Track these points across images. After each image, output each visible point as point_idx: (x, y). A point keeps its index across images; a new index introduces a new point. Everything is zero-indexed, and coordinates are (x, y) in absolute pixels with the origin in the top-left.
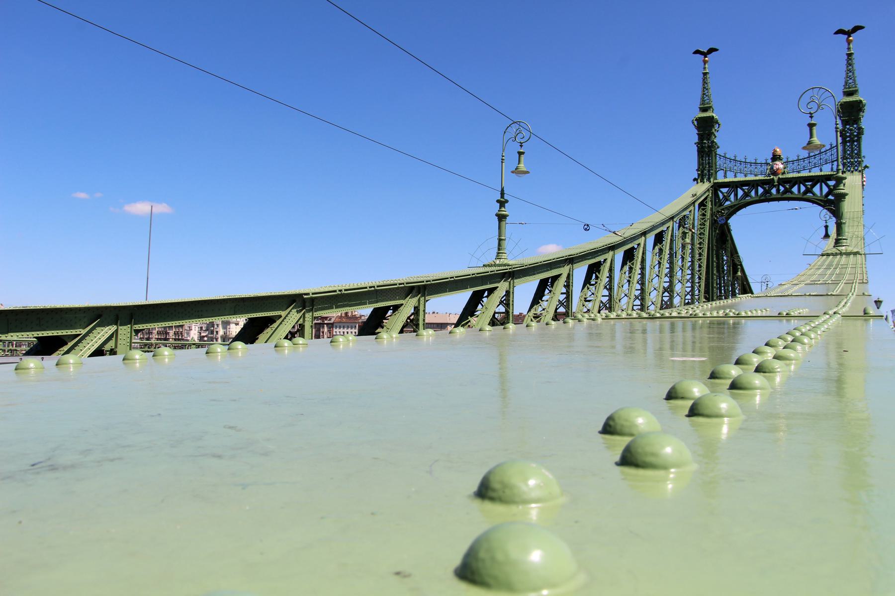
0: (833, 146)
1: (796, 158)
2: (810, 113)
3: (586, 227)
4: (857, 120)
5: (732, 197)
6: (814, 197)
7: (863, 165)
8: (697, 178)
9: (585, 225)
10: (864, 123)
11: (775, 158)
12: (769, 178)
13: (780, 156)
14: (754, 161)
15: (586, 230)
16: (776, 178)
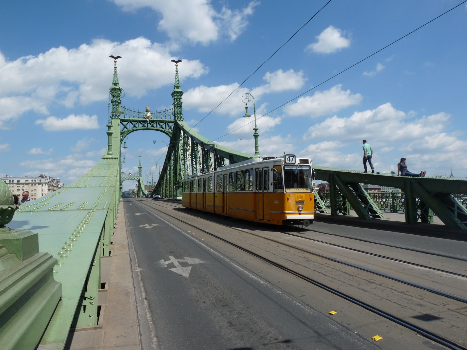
1: (156, 112)
2: (246, 103)
3: (154, 142)
4: (180, 99)
5: (127, 126)
7: (183, 118)
8: (112, 116)
9: (154, 141)
10: (182, 100)
11: (147, 111)
12: (145, 119)
13: (149, 110)
14: (138, 111)
15: (154, 143)
16: (148, 120)
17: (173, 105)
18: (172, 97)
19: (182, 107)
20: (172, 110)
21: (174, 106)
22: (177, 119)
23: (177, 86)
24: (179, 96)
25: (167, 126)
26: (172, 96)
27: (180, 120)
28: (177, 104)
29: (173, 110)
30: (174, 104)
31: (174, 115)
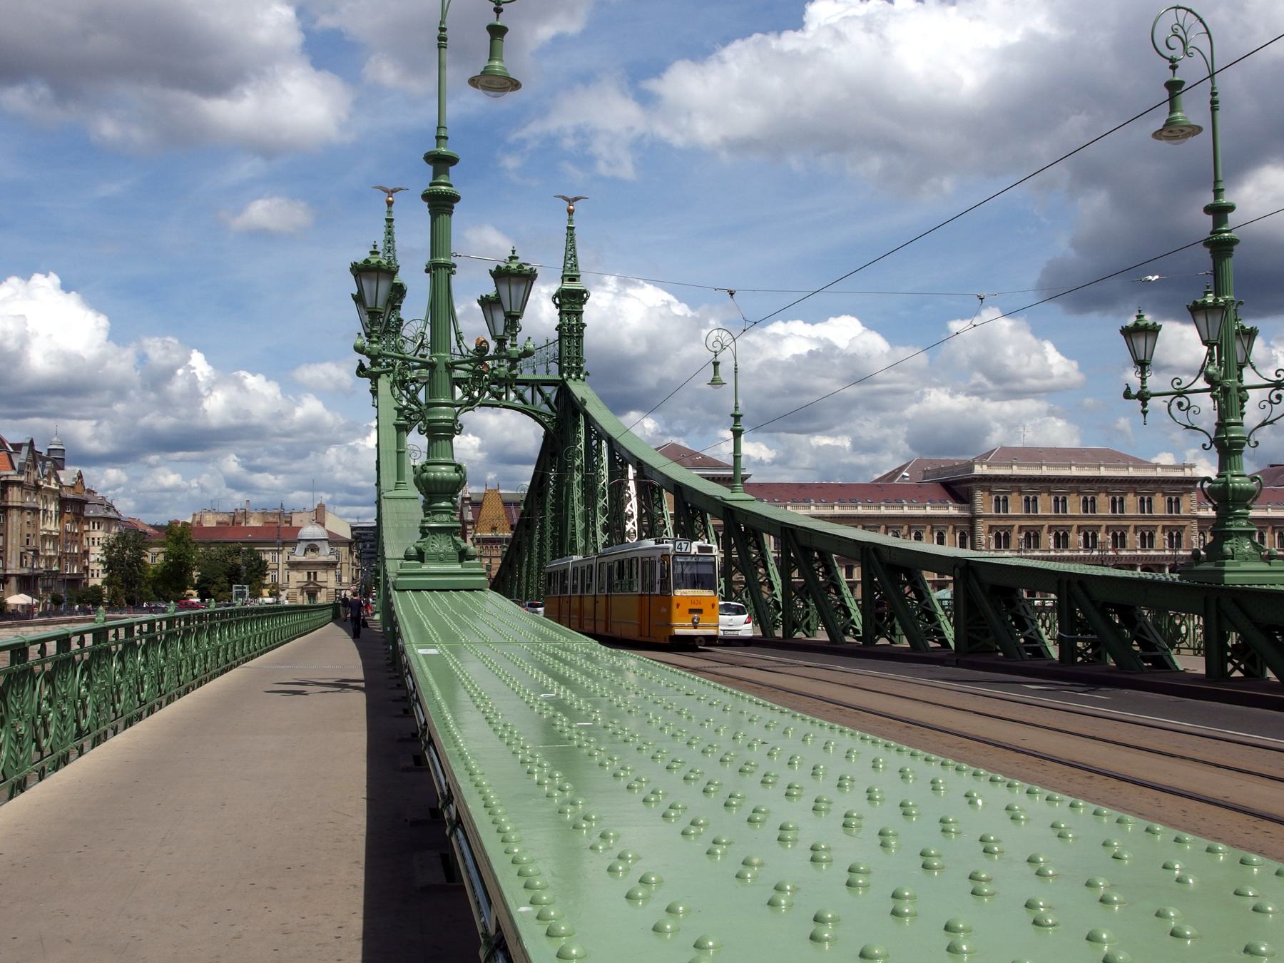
0: (550, 342)
6: (526, 406)
7: (585, 371)
10: (585, 318)
17: (556, 329)
18: (554, 305)
19: (584, 338)
20: (554, 346)
21: (559, 333)
22: (569, 375)
23: (570, 274)
24: (578, 306)
25: (538, 397)
26: (555, 302)
27: (575, 380)
28: (570, 330)
29: (557, 346)
30: (559, 328)
31: (558, 361)
